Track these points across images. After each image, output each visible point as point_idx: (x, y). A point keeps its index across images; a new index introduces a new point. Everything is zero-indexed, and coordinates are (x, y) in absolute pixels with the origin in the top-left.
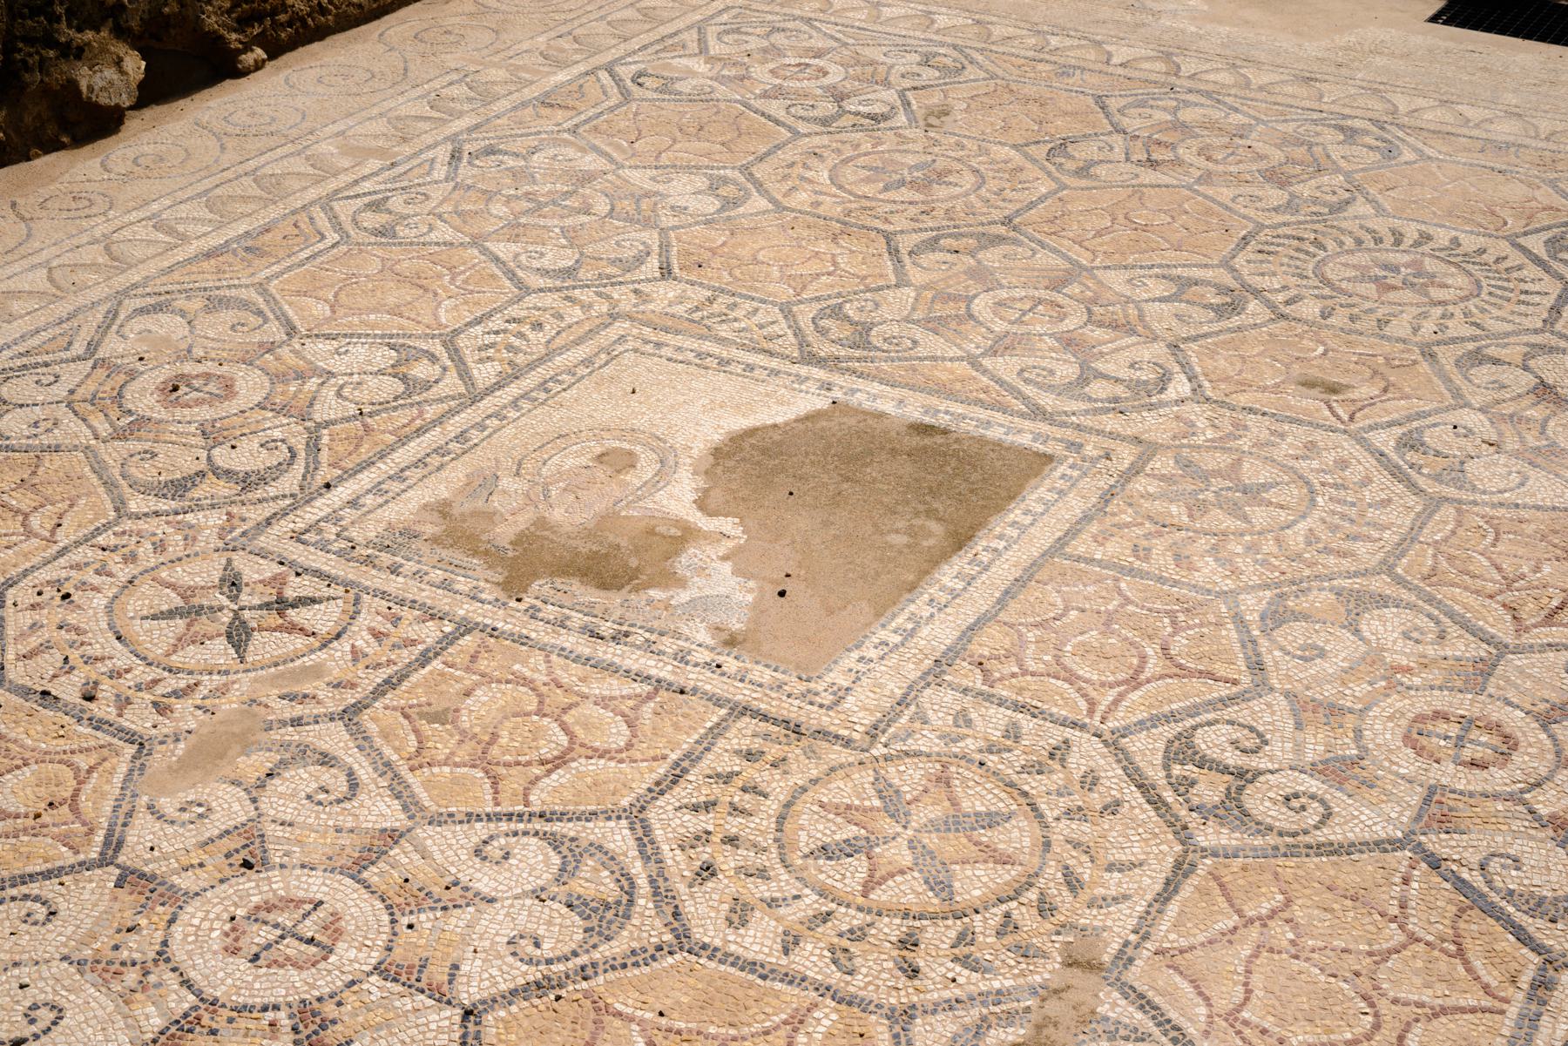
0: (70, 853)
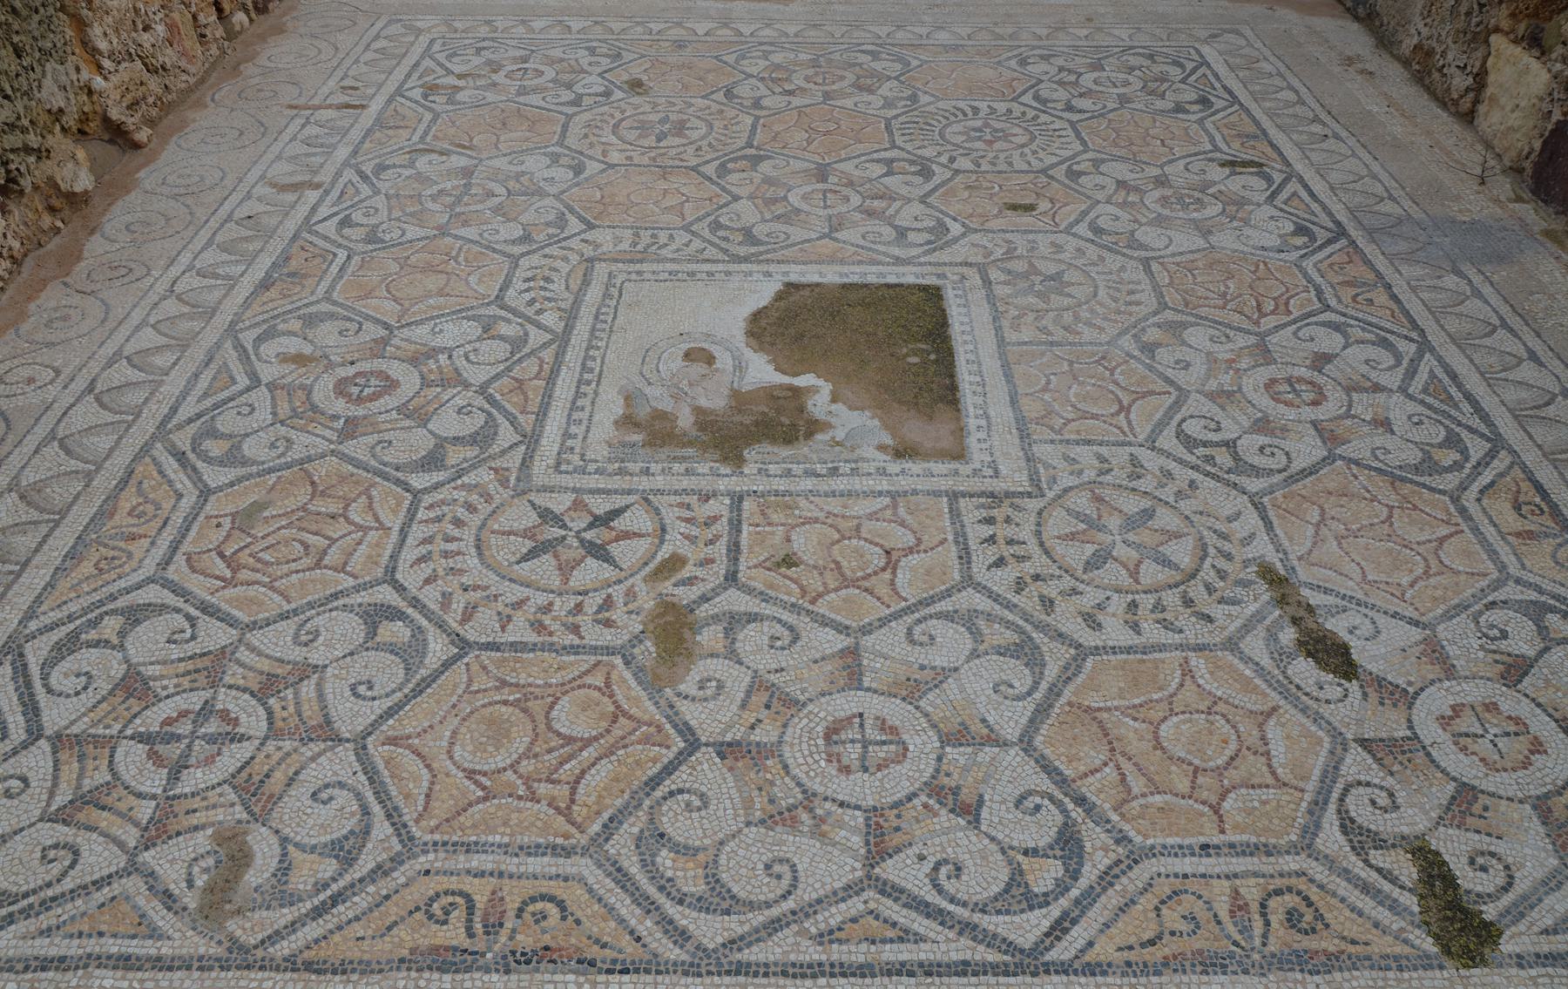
0: (664, 751)
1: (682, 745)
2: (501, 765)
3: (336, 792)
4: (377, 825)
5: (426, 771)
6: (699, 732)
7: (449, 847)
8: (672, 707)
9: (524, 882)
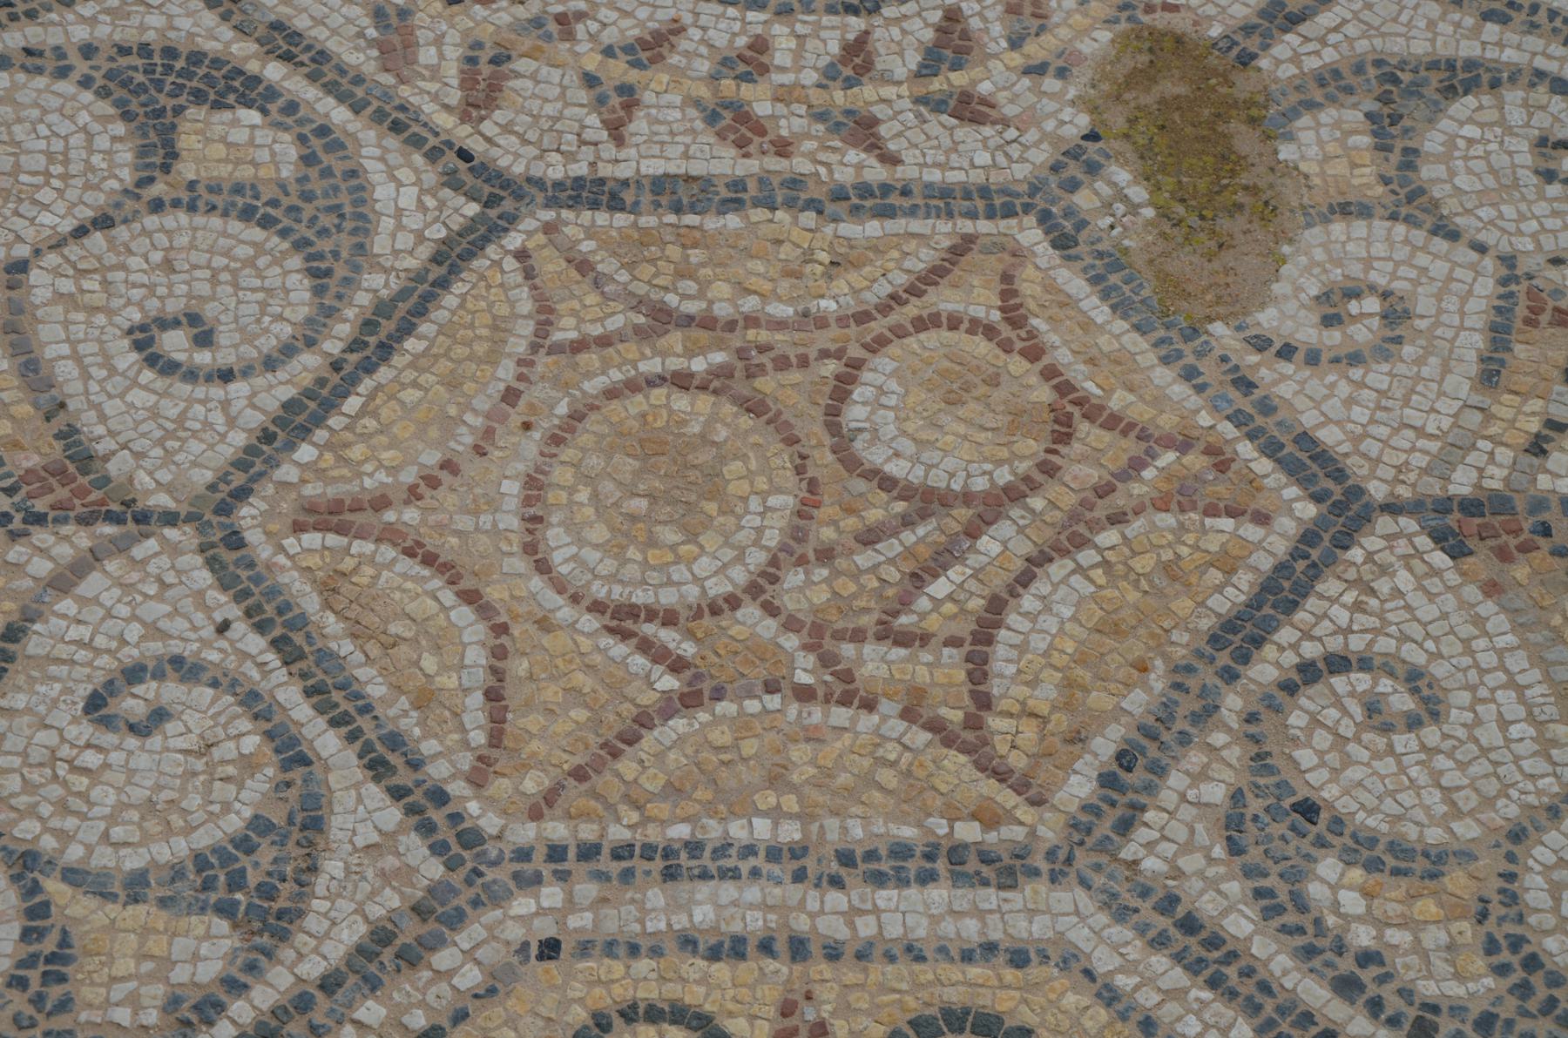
0: (1252, 532)
1: (1309, 510)
2: (718, 588)
3: (171, 691)
4: (344, 800)
5: (463, 614)
6: (1357, 467)
7: (605, 863)
8: (1245, 385)
9: (879, 971)
